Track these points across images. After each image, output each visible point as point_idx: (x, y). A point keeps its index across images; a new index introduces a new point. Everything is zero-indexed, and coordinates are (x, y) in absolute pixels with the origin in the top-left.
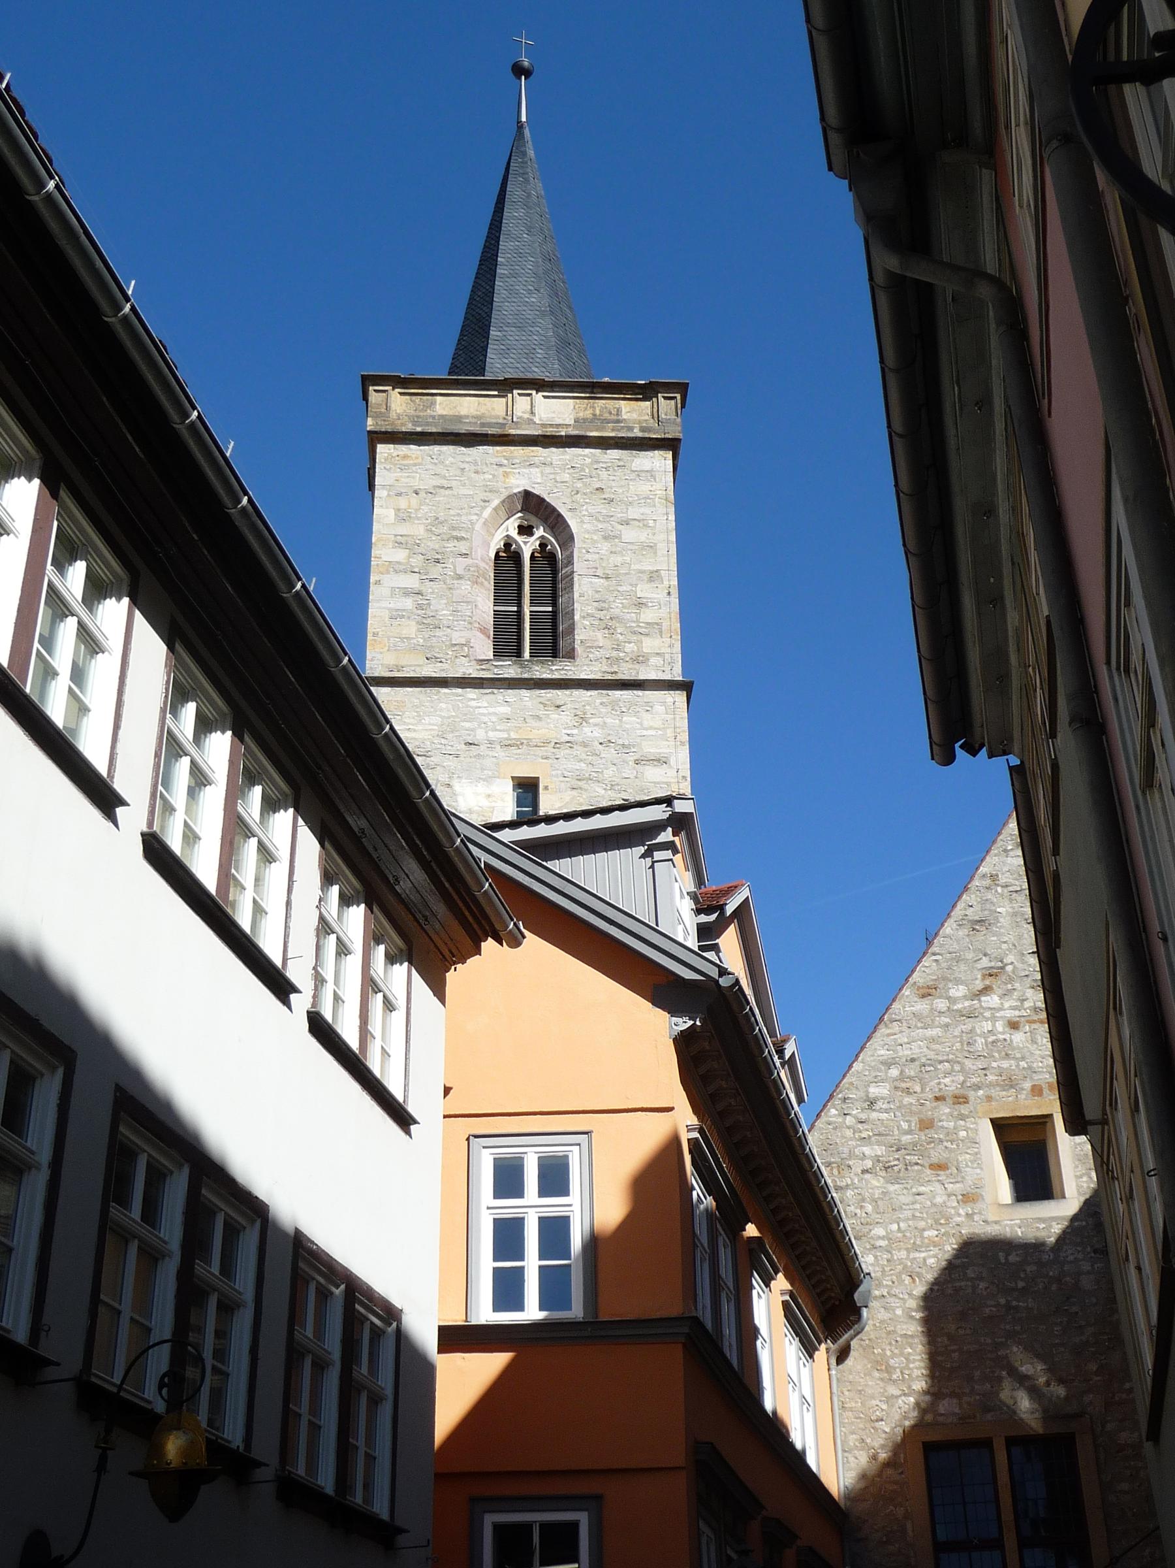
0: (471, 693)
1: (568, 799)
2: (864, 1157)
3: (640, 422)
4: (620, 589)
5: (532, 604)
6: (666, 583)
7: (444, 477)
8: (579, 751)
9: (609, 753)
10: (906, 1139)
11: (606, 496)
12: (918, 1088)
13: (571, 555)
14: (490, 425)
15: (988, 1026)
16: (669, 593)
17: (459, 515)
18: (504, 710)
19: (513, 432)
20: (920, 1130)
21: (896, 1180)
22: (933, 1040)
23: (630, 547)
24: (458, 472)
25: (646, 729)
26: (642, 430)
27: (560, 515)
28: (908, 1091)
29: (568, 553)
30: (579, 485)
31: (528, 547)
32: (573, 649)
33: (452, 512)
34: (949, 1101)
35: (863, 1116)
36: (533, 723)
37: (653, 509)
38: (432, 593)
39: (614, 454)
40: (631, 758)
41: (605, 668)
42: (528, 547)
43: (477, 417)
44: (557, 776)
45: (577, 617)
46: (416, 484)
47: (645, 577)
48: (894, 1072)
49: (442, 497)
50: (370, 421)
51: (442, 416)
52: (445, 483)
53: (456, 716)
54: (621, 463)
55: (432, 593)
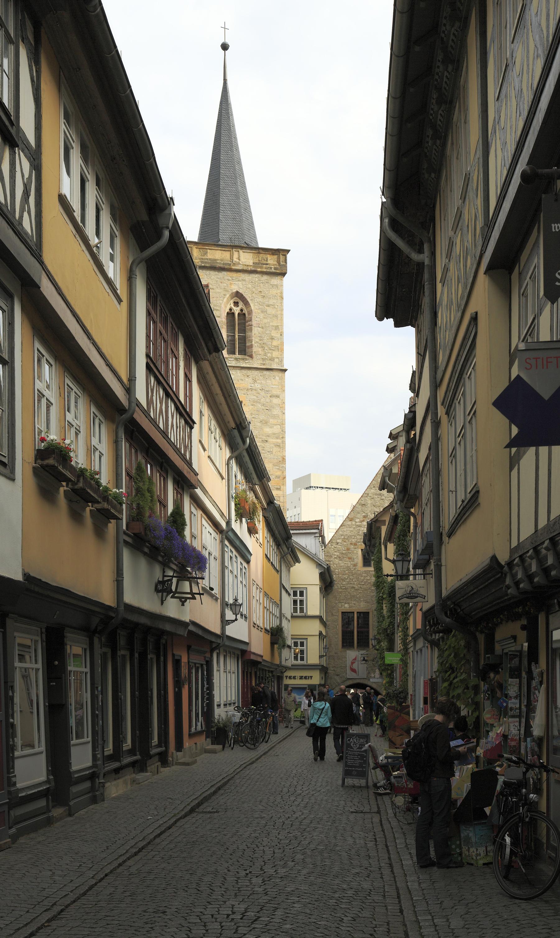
8: (254, 392)
9: (263, 393)
10: (344, 552)
11: (262, 294)
13: (251, 318)
14: (226, 264)
15: (363, 529)
19: (233, 267)
21: (341, 560)
22: (352, 531)
24: (216, 282)
28: (345, 542)
30: (254, 290)
31: (237, 310)
36: (241, 382)
39: (265, 277)
40: (269, 395)
41: (262, 362)
42: (237, 310)
43: (222, 260)
45: (253, 343)
47: (274, 328)
48: (343, 537)
51: (210, 259)
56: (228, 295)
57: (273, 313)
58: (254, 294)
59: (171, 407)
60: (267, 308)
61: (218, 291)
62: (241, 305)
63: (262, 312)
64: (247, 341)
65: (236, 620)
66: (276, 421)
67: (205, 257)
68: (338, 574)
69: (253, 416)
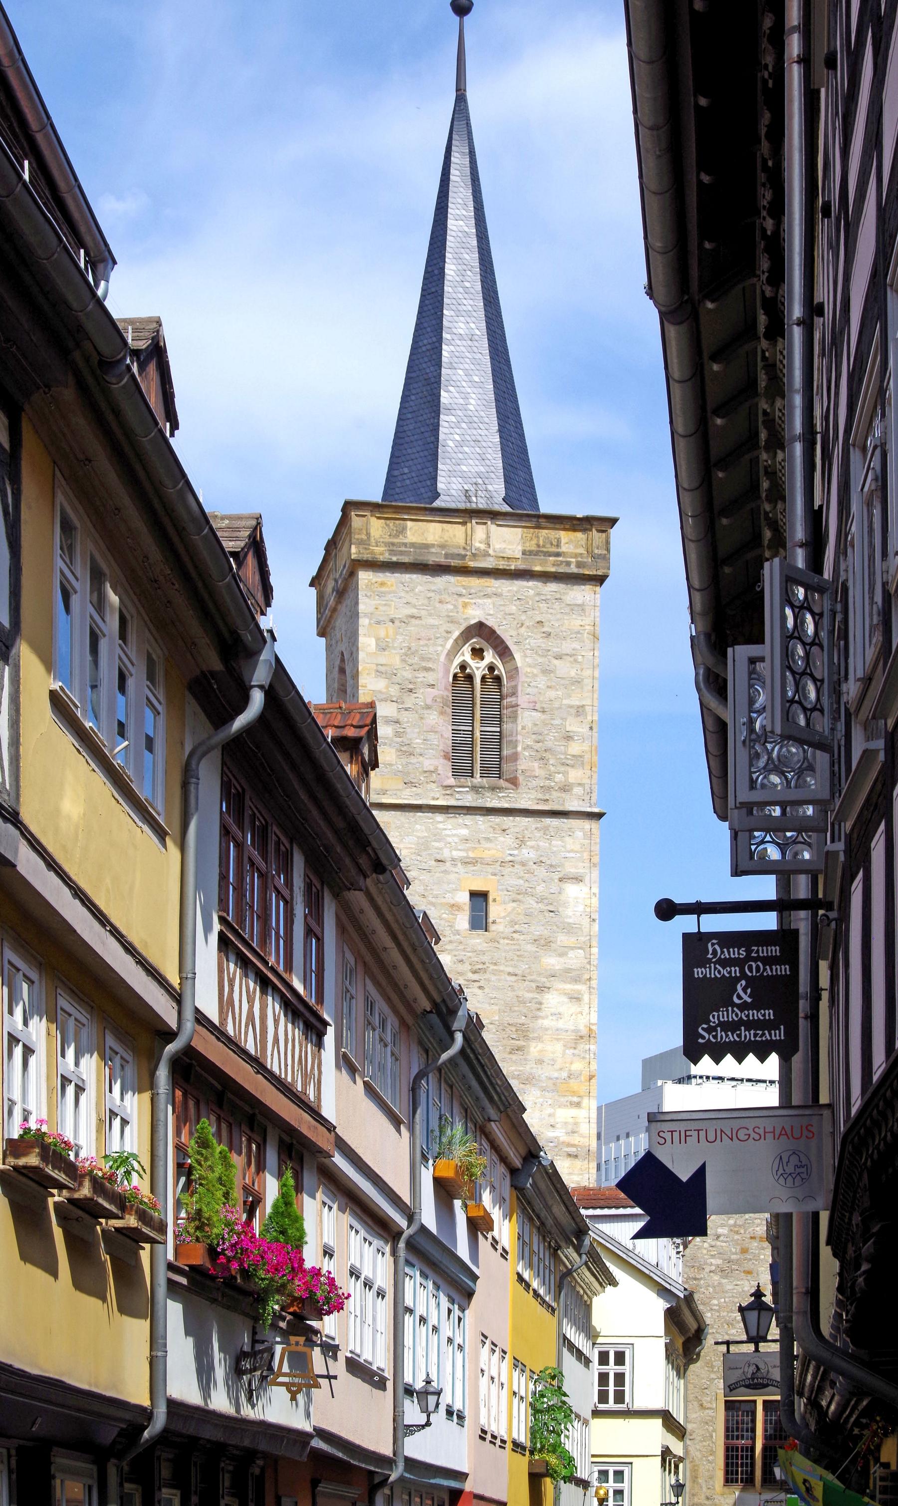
0: (439, 817)
1: (509, 909)
2: (711, 1264)
3: (576, 556)
4: (552, 722)
5: (482, 723)
6: (589, 718)
7: (415, 606)
9: (541, 872)
11: (545, 629)
12: (742, 1231)
13: (515, 687)
16: (591, 728)
17: (426, 645)
18: (464, 832)
19: (472, 564)
20: (741, 1253)
21: (726, 1277)
23: (562, 682)
24: (426, 602)
25: (569, 852)
26: (579, 565)
27: (507, 648)
28: (737, 1233)
29: (513, 684)
30: (523, 617)
31: (478, 668)
32: (516, 778)
33: (422, 643)
34: (758, 1240)
35: (713, 1243)
37: (582, 644)
38: (408, 722)
39: (553, 587)
40: (556, 876)
41: (540, 796)
42: (478, 668)
43: (442, 546)
44: (502, 890)
45: (519, 749)
46: (393, 613)
47: (573, 711)
49: (413, 628)
50: (354, 549)
51: (413, 545)
52: (414, 611)
53: (429, 837)
54: (558, 596)
55: (408, 722)
56: (456, 634)
57: (573, 673)
58: (523, 630)
59: (274, 1007)
60: (556, 662)
61: (431, 621)
62: (490, 656)
63: (545, 672)
64: (504, 746)
65: (428, 1424)
66: (573, 939)
67: (401, 539)
68: (718, 1311)
69: (517, 927)
